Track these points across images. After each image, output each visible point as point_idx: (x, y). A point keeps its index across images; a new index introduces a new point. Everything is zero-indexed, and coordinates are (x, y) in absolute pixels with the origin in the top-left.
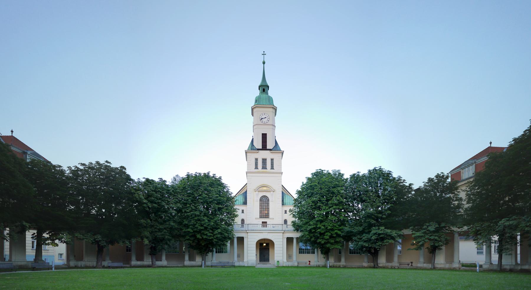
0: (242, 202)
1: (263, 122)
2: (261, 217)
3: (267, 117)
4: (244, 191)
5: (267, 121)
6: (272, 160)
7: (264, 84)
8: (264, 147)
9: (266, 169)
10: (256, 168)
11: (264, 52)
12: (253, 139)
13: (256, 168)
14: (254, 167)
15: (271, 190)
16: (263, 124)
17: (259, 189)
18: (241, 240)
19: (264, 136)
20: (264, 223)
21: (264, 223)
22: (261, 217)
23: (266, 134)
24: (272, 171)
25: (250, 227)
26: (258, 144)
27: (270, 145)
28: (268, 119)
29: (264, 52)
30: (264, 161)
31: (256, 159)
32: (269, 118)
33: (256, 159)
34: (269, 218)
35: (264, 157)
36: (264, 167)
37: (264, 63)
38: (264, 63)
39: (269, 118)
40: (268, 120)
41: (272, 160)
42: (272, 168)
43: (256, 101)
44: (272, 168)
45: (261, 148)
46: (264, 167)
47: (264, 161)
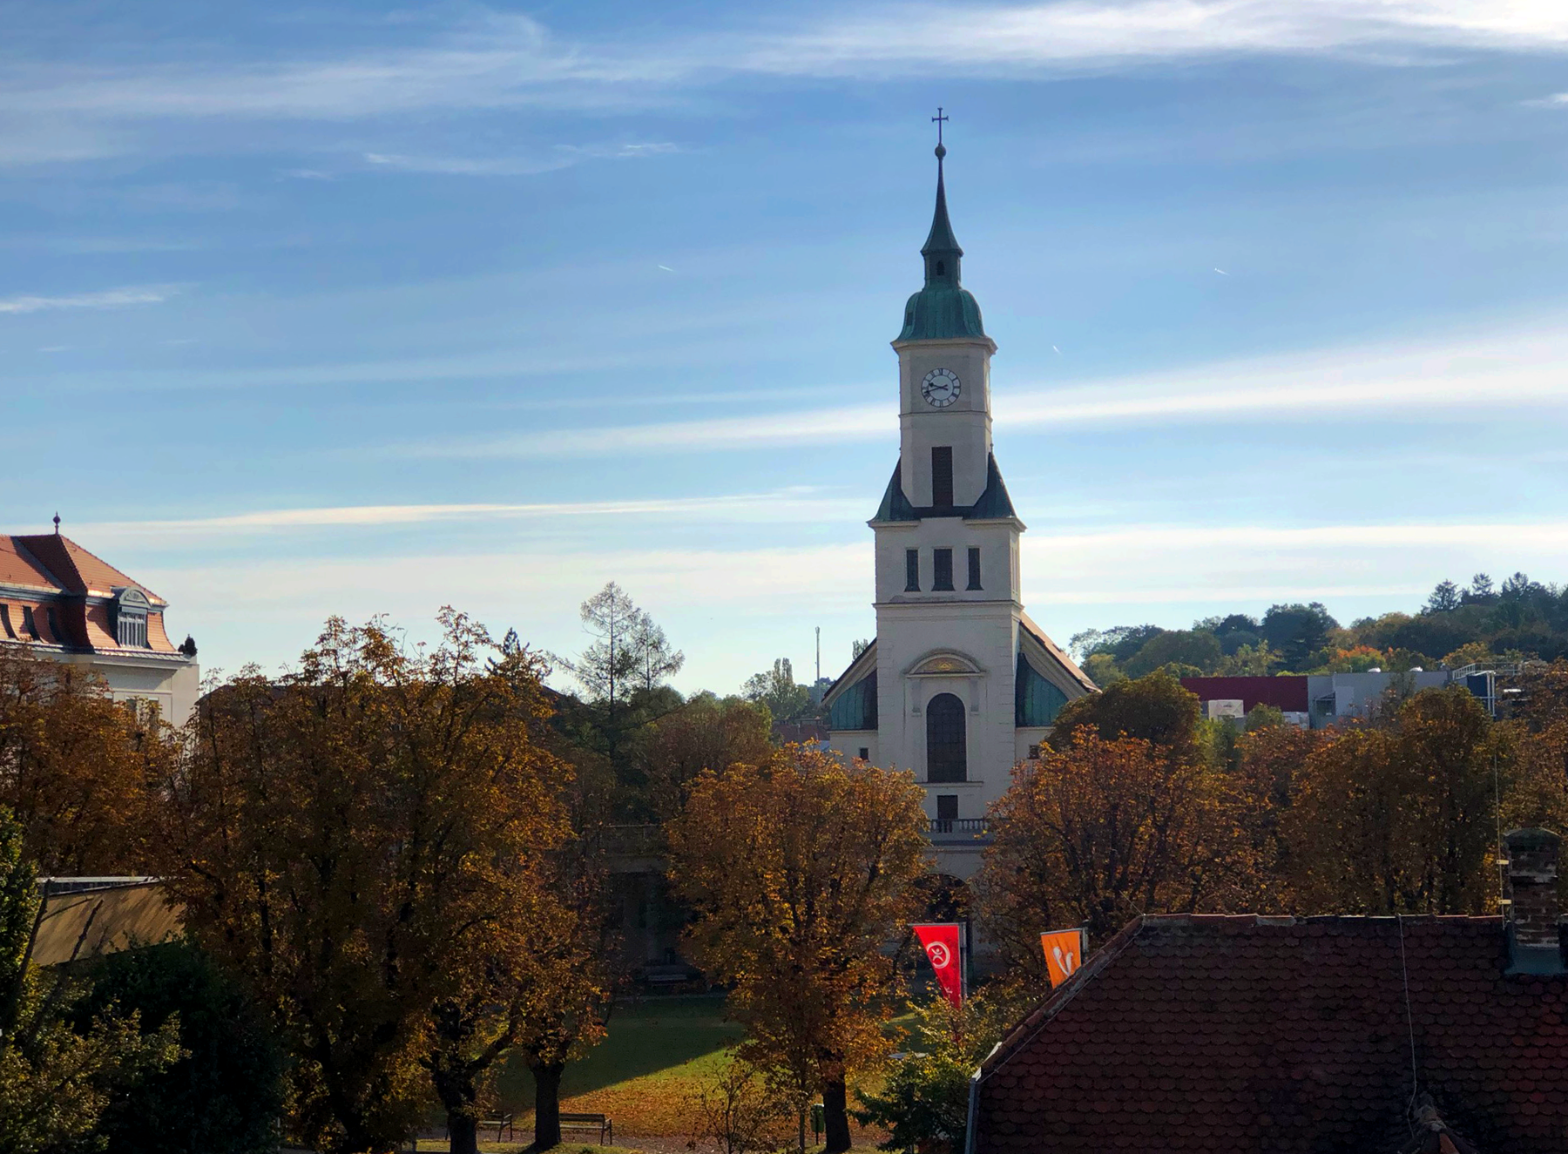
0: (860, 717)
1: (937, 403)
2: (935, 777)
3: (950, 387)
4: (860, 674)
5: (952, 399)
6: (974, 554)
8: (943, 505)
9: (952, 589)
10: (912, 585)
11: (940, 110)
13: (912, 585)
14: (904, 584)
15: (968, 667)
16: (931, 408)
17: (922, 668)
19: (942, 460)
20: (948, 807)
21: (948, 807)
22: (935, 777)
23: (950, 448)
26: (920, 494)
27: (966, 491)
28: (957, 391)
29: (940, 110)
30: (943, 558)
31: (912, 555)
32: (959, 387)
33: (912, 555)
34: (963, 780)
36: (943, 580)
37: (940, 152)
39: (959, 387)
40: (953, 394)
41: (974, 554)
42: (974, 583)
44: (974, 583)
45: (927, 500)
46: (943, 580)
47: (943, 558)
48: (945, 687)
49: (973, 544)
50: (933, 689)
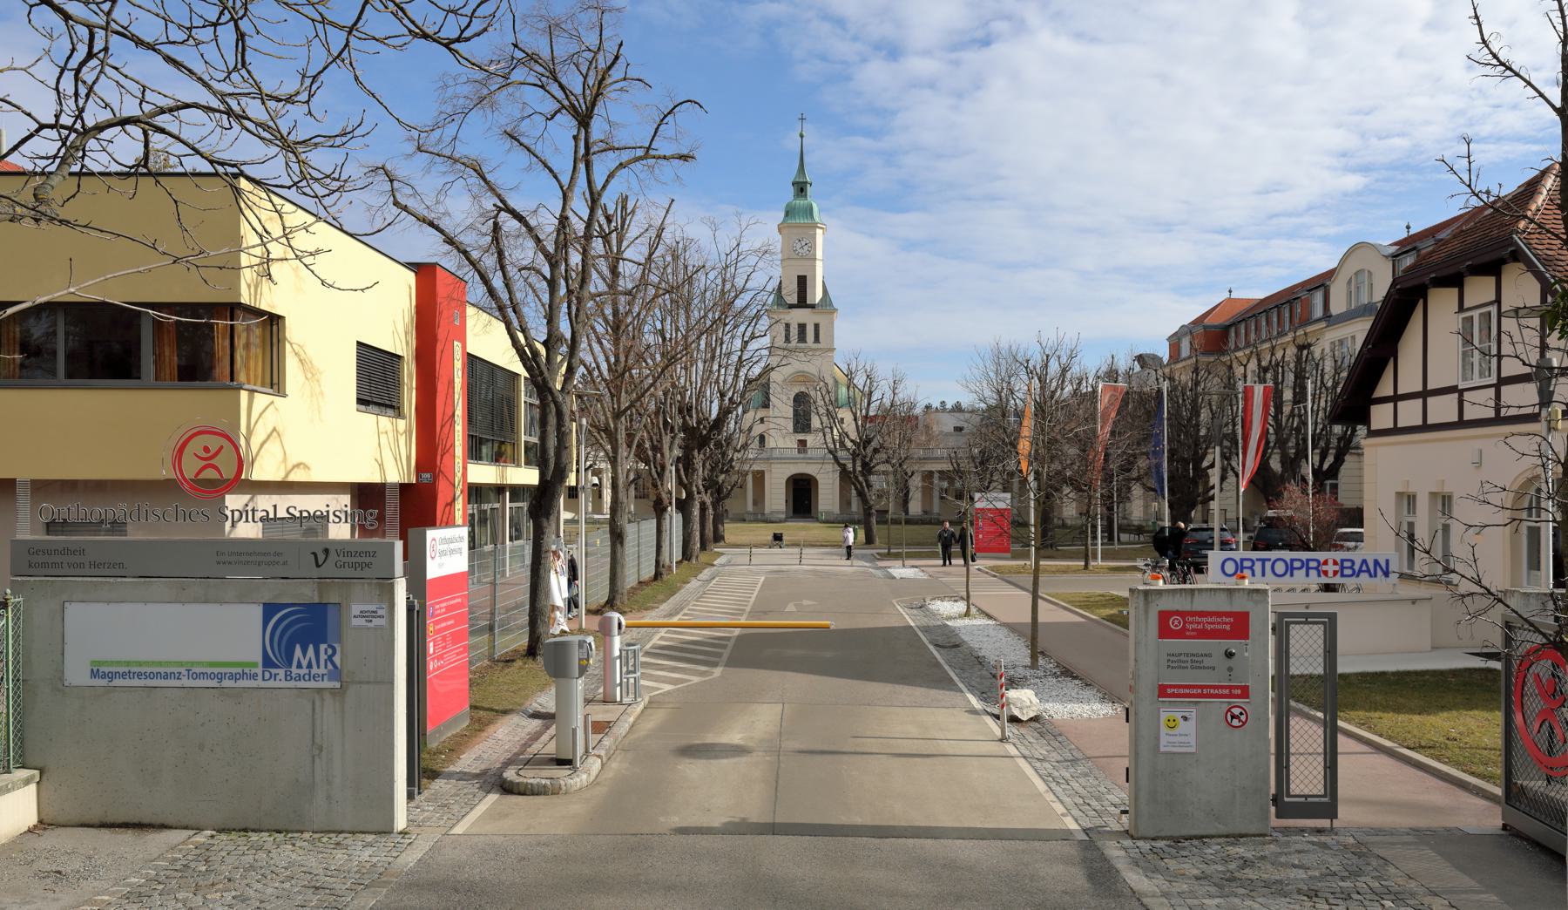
2: (796, 431)
6: (817, 326)
7: (801, 180)
8: (802, 302)
10: (787, 339)
12: (780, 283)
18: (759, 477)
19: (802, 282)
20: (803, 443)
21: (803, 443)
22: (796, 431)
24: (816, 346)
25: (776, 454)
30: (802, 328)
35: (802, 322)
38: (802, 136)
41: (817, 326)
42: (817, 339)
43: (787, 214)
44: (817, 339)
46: (802, 337)
47: (802, 328)
48: (803, 389)
49: (816, 322)
50: (796, 390)
